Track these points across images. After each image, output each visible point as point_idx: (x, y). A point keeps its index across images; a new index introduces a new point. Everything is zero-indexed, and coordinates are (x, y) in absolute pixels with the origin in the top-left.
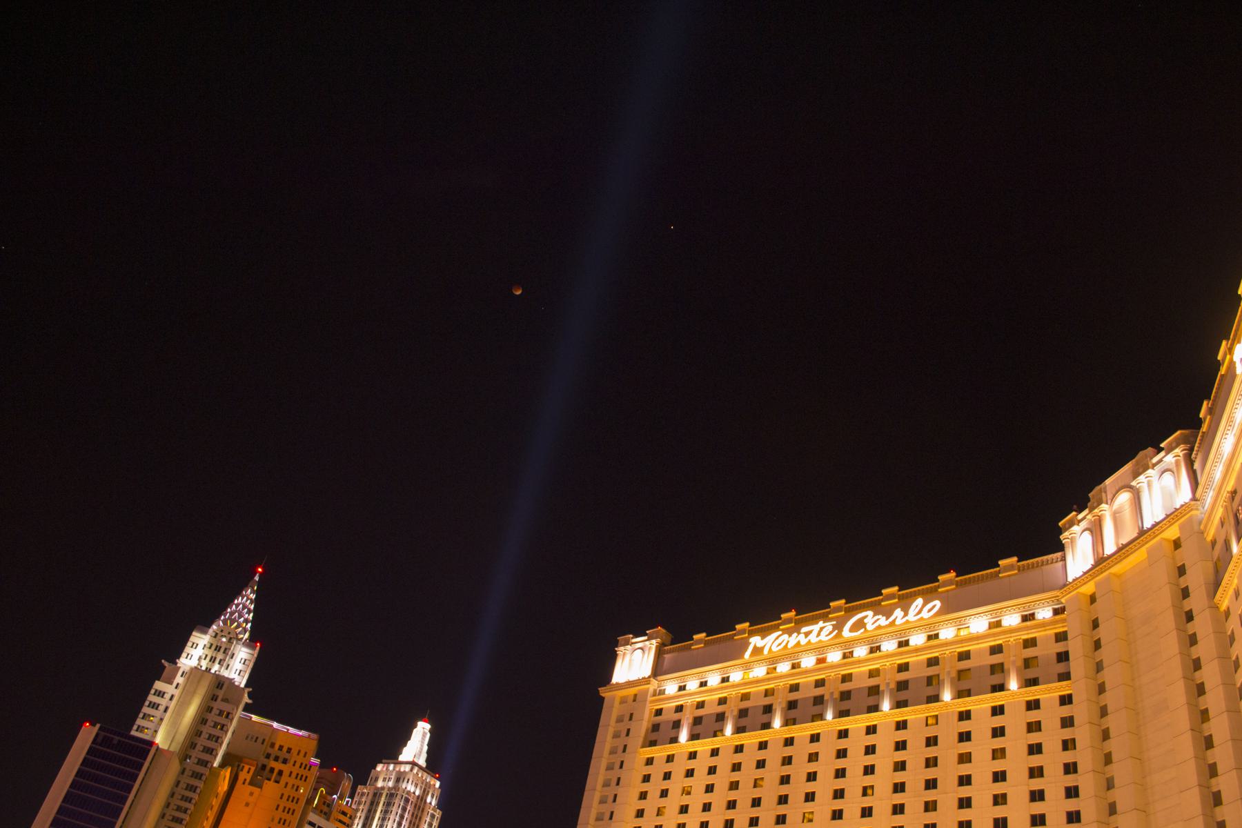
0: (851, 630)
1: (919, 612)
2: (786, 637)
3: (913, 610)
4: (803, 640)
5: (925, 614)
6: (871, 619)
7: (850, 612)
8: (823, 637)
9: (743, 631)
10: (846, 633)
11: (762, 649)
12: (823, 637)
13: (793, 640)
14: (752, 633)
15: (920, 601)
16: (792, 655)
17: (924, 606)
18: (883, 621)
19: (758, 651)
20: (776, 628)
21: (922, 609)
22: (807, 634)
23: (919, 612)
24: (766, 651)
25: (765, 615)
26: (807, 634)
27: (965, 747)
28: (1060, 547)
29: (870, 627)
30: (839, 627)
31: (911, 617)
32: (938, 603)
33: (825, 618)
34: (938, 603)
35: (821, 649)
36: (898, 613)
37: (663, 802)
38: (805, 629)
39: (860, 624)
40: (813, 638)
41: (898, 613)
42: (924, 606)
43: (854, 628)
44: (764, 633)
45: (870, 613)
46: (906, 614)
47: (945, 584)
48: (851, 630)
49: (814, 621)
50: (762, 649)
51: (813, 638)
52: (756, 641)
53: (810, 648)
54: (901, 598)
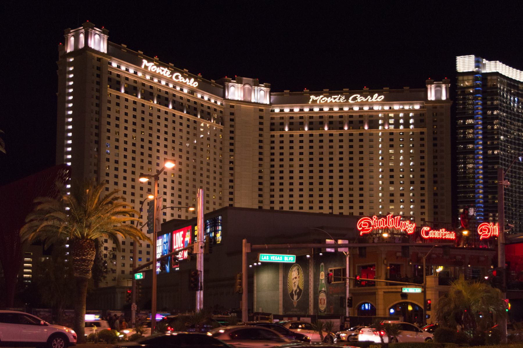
2: (326, 98)
5: (378, 100)
6: (360, 99)
8: (341, 100)
9: (306, 93)
10: (350, 101)
11: (316, 101)
13: (329, 100)
15: (376, 95)
17: (378, 96)
18: (364, 99)
19: (314, 101)
21: (377, 98)
22: (335, 99)
23: (376, 99)
24: (318, 102)
26: (335, 99)
27: (292, 151)
30: (347, 98)
31: (374, 100)
32: (383, 97)
34: (383, 97)
38: (333, 97)
39: (355, 99)
42: (378, 96)
43: (353, 100)
44: (317, 95)
45: (359, 96)
46: (372, 98)
50: (316, 101)
51: (337, 100)
52: (313, 97)
53: (336, 104)
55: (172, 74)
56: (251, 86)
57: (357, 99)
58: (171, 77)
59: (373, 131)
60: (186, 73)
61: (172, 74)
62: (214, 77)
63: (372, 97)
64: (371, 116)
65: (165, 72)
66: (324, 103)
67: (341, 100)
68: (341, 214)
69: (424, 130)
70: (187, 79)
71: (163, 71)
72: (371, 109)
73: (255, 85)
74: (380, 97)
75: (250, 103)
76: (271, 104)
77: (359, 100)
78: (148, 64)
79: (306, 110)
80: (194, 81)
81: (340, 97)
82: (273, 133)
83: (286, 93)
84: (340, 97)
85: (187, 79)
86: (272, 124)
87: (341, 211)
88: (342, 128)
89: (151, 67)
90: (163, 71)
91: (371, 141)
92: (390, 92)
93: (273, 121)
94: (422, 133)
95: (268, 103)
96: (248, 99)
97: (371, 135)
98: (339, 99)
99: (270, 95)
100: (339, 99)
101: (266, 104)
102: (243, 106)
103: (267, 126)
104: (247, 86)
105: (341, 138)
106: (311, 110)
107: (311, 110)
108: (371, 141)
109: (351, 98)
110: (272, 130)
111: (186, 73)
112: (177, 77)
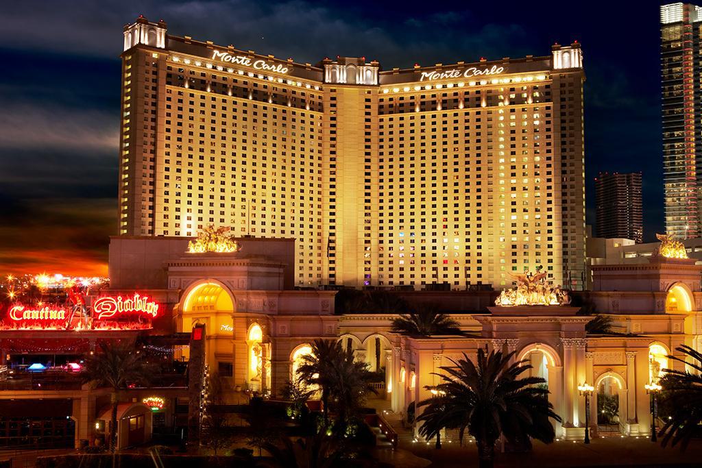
3: (492, 70)
7: (466, 67)
12: (455, 76)
14: (422, 71)
15: (495, 67)
17: (497, 68)
18: (480, 73)
20: (434, 70)
24: (430, 79)
25: (429, 66)
26: (448, 74)
28: (552, 55)
31: (492, 72)
33: (456, 68)
36: (487, 70)
38: (447, 72)
39: (471, 73)
40: (451, 76)
42: (497, 68)
44: (428, 71)
46: (490, 71)
47: (505, 61)
49: (451, 69)
54: (487, 64)
55: (252, 62)
58: (252, 66)
59: (492, 109)
61: (252, 62)
63: (490, 69)
64: (490, 92)
66: (435, 82)
69: (550, 104)
71: (240, 60)
73: (360, 65)
74: (499, 69)
75: (355, 85)
76: (379, 84)
78: (219, 55)
80: (283, 67)
82: (381, 117)
85: (273, 67)
86: (381, 107)
89: (224, 56)
90: (240, 60)
91: (490, 120)
92: (510, 62)
93: (382, 103)
94: (548, 108)
95: (376, 83)
96: (351, 81)
97: (490, 113)
99: (378, 74)
101: (374, 85)
102: (346, 89)
104: (351, 66)
105: (456, 118)
108: (490, 120)
109: (466, 73)
110: (381, 113)
112: (259, 65)
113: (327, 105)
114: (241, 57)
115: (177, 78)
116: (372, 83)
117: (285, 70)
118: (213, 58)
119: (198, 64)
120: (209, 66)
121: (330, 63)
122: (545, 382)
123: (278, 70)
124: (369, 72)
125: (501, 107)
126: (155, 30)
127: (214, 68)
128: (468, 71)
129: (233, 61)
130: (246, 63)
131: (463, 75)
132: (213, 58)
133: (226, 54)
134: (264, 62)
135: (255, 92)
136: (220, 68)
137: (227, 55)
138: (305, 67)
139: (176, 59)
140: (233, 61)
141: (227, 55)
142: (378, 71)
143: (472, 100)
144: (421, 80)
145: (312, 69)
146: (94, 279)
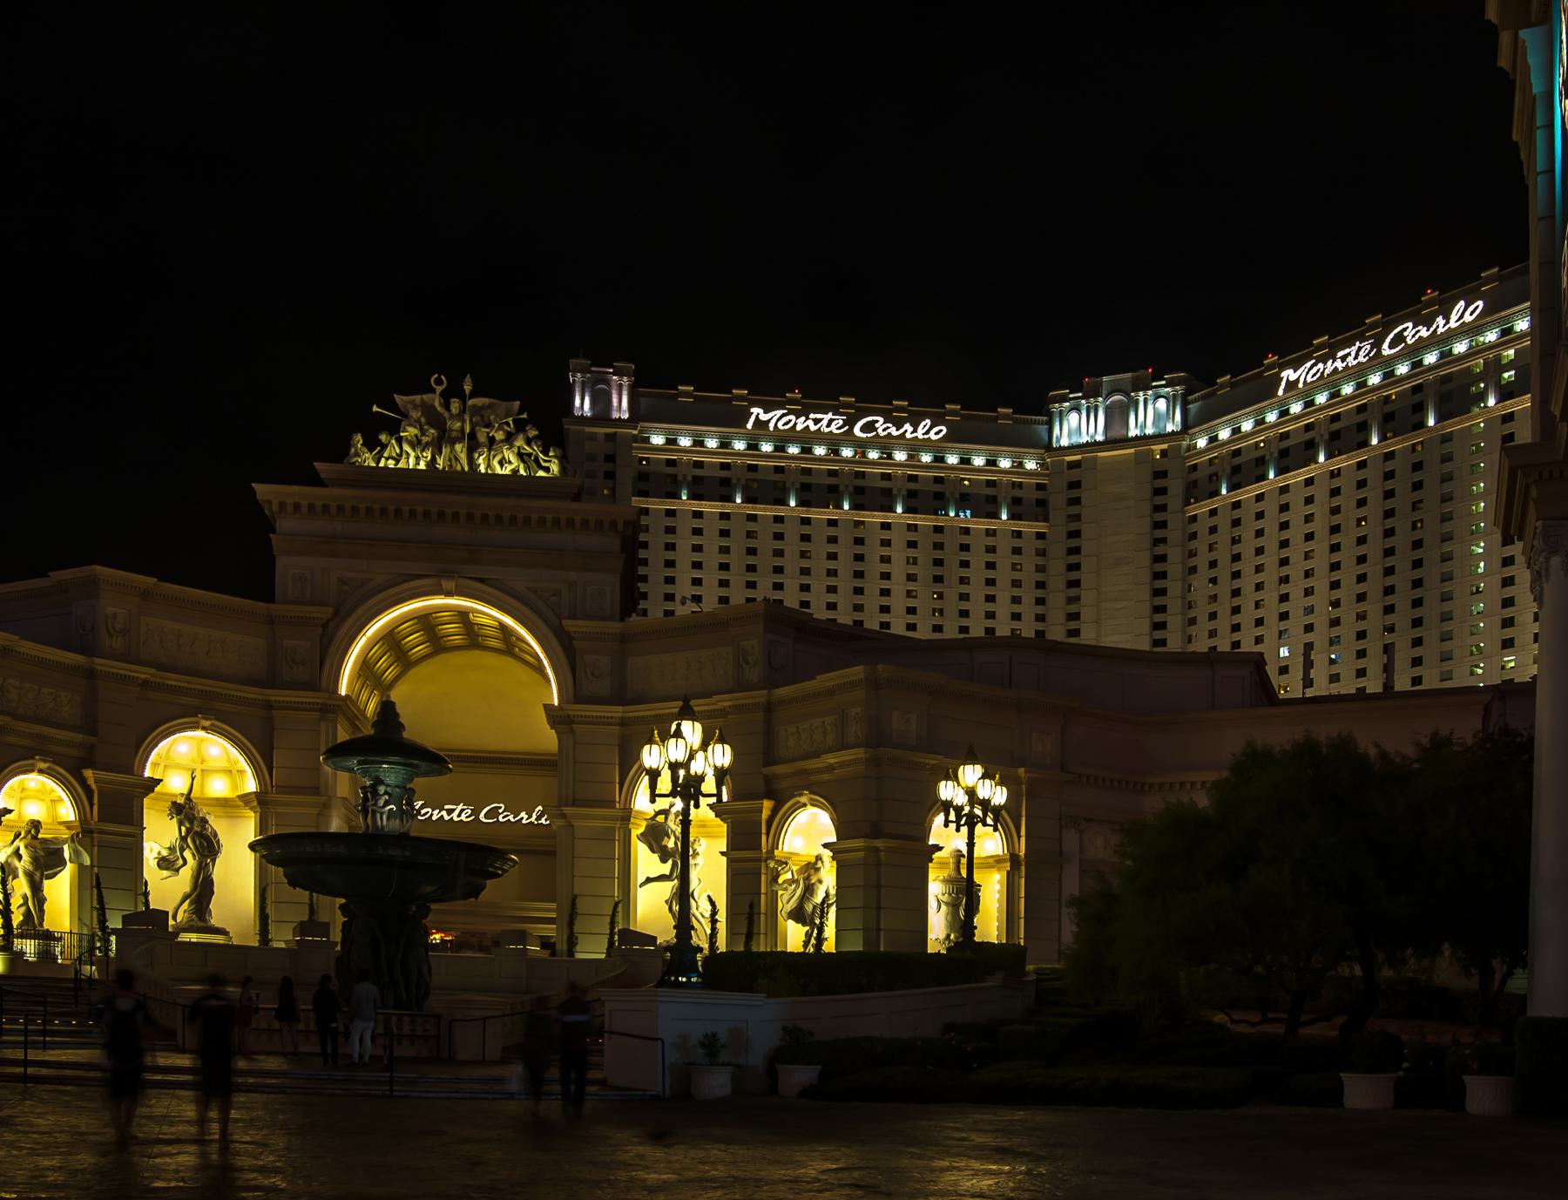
0: (1391, 347)
1: (1461, 317)
3: (1454, 317)
4: (1339, 365)
5: (1468, 318)
6: (1412, 332)
9: (1271, 367)
10: (1386, 351)
14: (1283, 367)
16: (1331, 383)
18: (1424, 333)
19: (1292, 385)
21: (1463, 313)
22: (1343, 359)
23: (1461, 317)
26: (1343, 359)
29: (1410, 341)
30: (1377, 345)
35: (1358, 373)
37: (1213, 538)
38: (1340, 354)
39: (1400, 338)
41: (1440, 321)
45: (1410, 325)
47: (1487, 281)
48: (1391, 347)
51: (1351, 361)
52: (1289, 374)
56: (1127, 394)
57: (1404, 339)
60: (900, 409)
61: (850, 422)
62: (1007, 396)
65: (829, 423)
66: (1310, 383)
67: (833, 428)
68: (1361, 690)
70: (908, 427)
71: (817, 421)
72: (1446, 355)
73: (1136, 390)
75: (1125, 441)
77: (1410, 341)
78: (764, 417)
79: (1271, 417)
81: (831, 421)
83: (1222, 386)
84: (831, 421)
87: (1361, 683)
88: (1365, 443)
89: (776, 419)
96: (1116, 433)
98: (828, 426)
100: (828, 426)
103: (1176, 487)
106: (1284, 413)
107: (1284, 413)
109: (1386, 345)
111: (900, 409)
113: (1057, 501)
114: (819, 416)
115: (665, 478)
116: (1170, 428)
117: (938, 433)
118: (749, 426)
119: (712, 443)
120: (740, 445)
121: (1064, 399)
122: (10, 811)
123: (920, 434)
124: (1162, 404)
125: (1478, 416)
126: (608, 382)
127: (753, 447)
128: (1388, 340)
129: (799, 427)
130: (833, 428)
131: (1379, 351)
132: (749, 426)
133: (779, 413)
134: (881, 420)
135: (859, 491)
136: (767, 448)
137: (784, 415)
138: (997, 418)
139: (658, 440)
140: (799, 427)
141: (784, 415)
142: (1184, 396)
143: (1397, 413)
144: (1280, 392)
145: (1016, 421)
146: (323, 900)
